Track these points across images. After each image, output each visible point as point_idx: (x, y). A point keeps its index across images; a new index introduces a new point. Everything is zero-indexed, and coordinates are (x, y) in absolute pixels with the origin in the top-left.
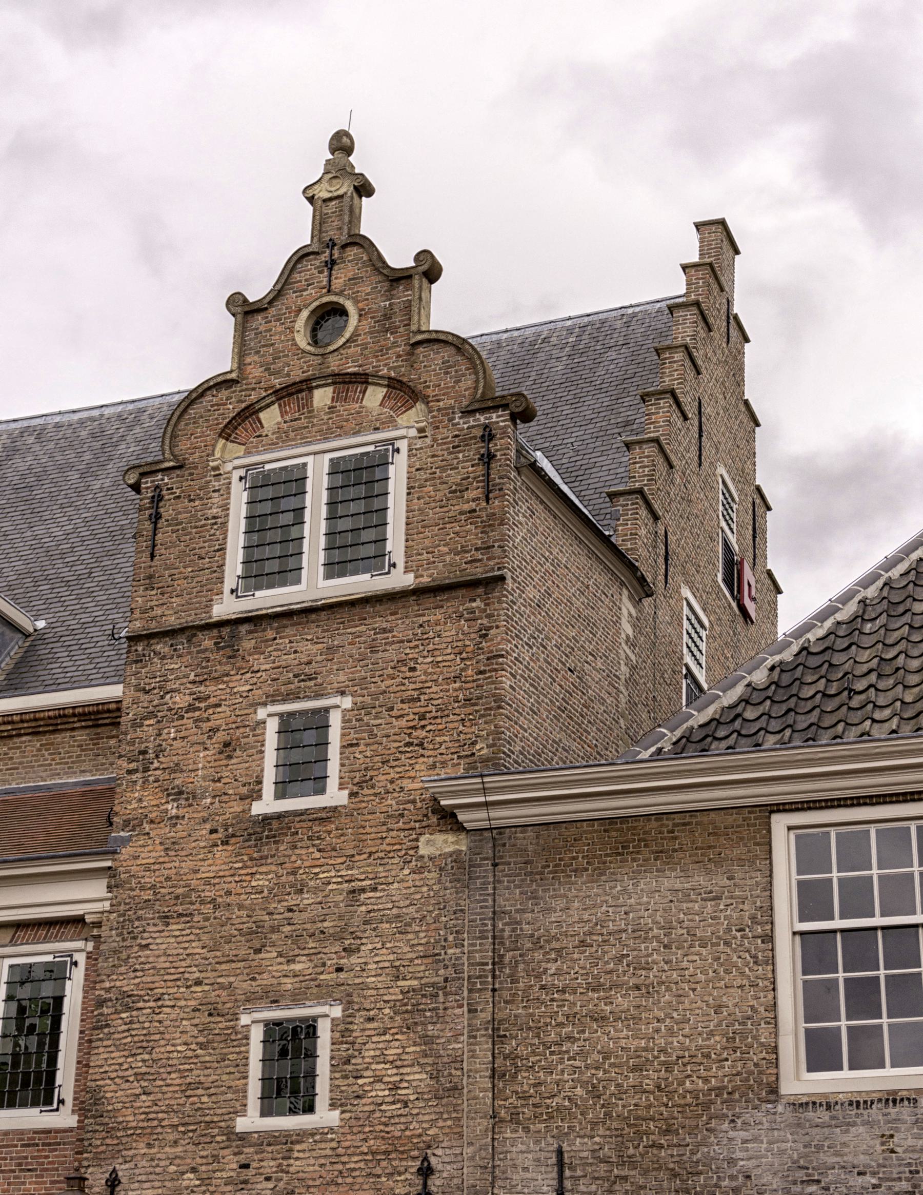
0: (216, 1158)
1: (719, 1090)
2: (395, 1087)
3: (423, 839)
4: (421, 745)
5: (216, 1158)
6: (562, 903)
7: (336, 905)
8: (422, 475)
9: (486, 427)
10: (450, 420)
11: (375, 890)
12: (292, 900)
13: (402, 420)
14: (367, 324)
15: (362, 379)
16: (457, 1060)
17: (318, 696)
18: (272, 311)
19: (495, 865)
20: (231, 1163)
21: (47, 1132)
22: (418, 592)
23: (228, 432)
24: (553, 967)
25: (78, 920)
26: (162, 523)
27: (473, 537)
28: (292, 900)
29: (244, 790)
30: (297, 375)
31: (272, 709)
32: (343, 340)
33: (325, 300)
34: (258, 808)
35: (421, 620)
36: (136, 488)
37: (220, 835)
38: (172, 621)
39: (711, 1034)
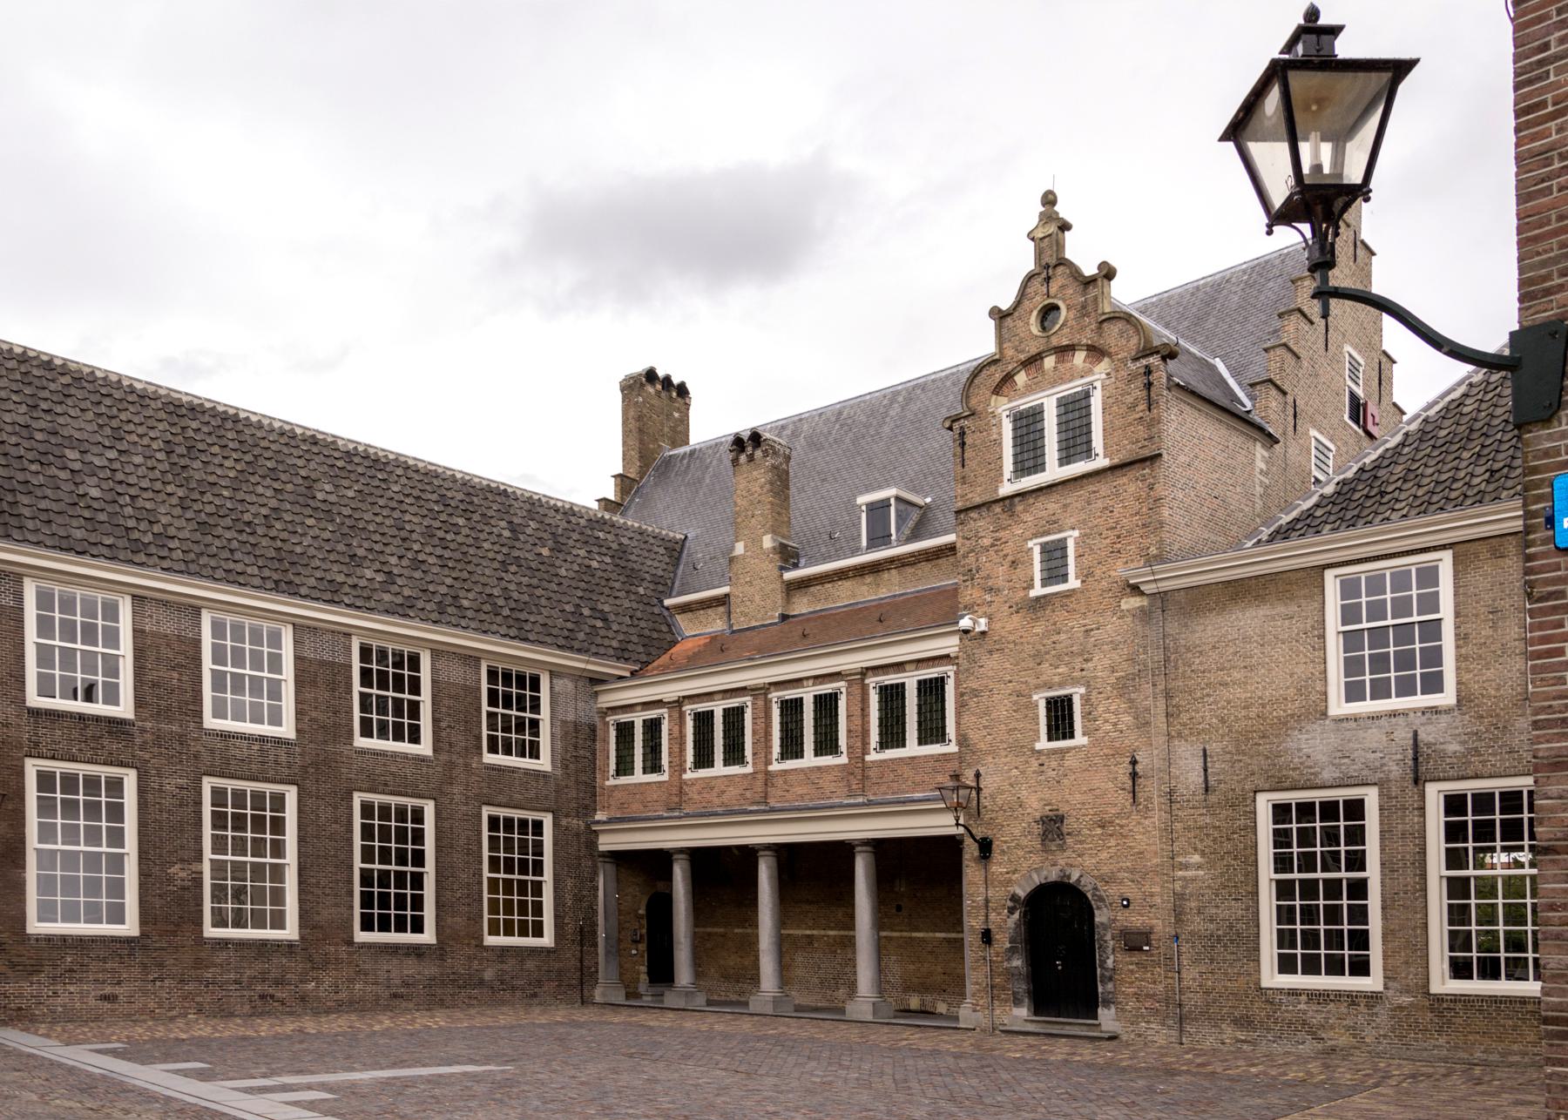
0: (1027, 762)
1: (1292, 716)
2: (1115, 724)
3: (1123, 601)
4: (1119, 552)
5: (1027, 762)
6: (1202, 627)
7: (1078, 638)
8: (1111, 400)
9: (1146, 367)
10: (1125, 365)
11: (1098, 629)
12: (1055, 638)
13: (1097, 369)
15: (1071, 348)
16: (1148, 710)
17: (1060, 531)
18: (1016, 314)
19: (1163, 611)
20: (1035, 764)
21: (945, 754)
22: (1112, 469)
23: (997, 390)
24: (1197, 661)
25: (947, 656)
26: (966, 447)
27: (1141, 431)
28: (1055, 638)
29: (1025, 585)
30: (1034, 351)
31: (1035, 541)
32: (1057, 327)
33: (1046, 302)
34: (1033, 593)
35: (1115, 484)
36: (950, 428)
37: (1015, 608)
38: (978, 500)
39: (1288, 688)
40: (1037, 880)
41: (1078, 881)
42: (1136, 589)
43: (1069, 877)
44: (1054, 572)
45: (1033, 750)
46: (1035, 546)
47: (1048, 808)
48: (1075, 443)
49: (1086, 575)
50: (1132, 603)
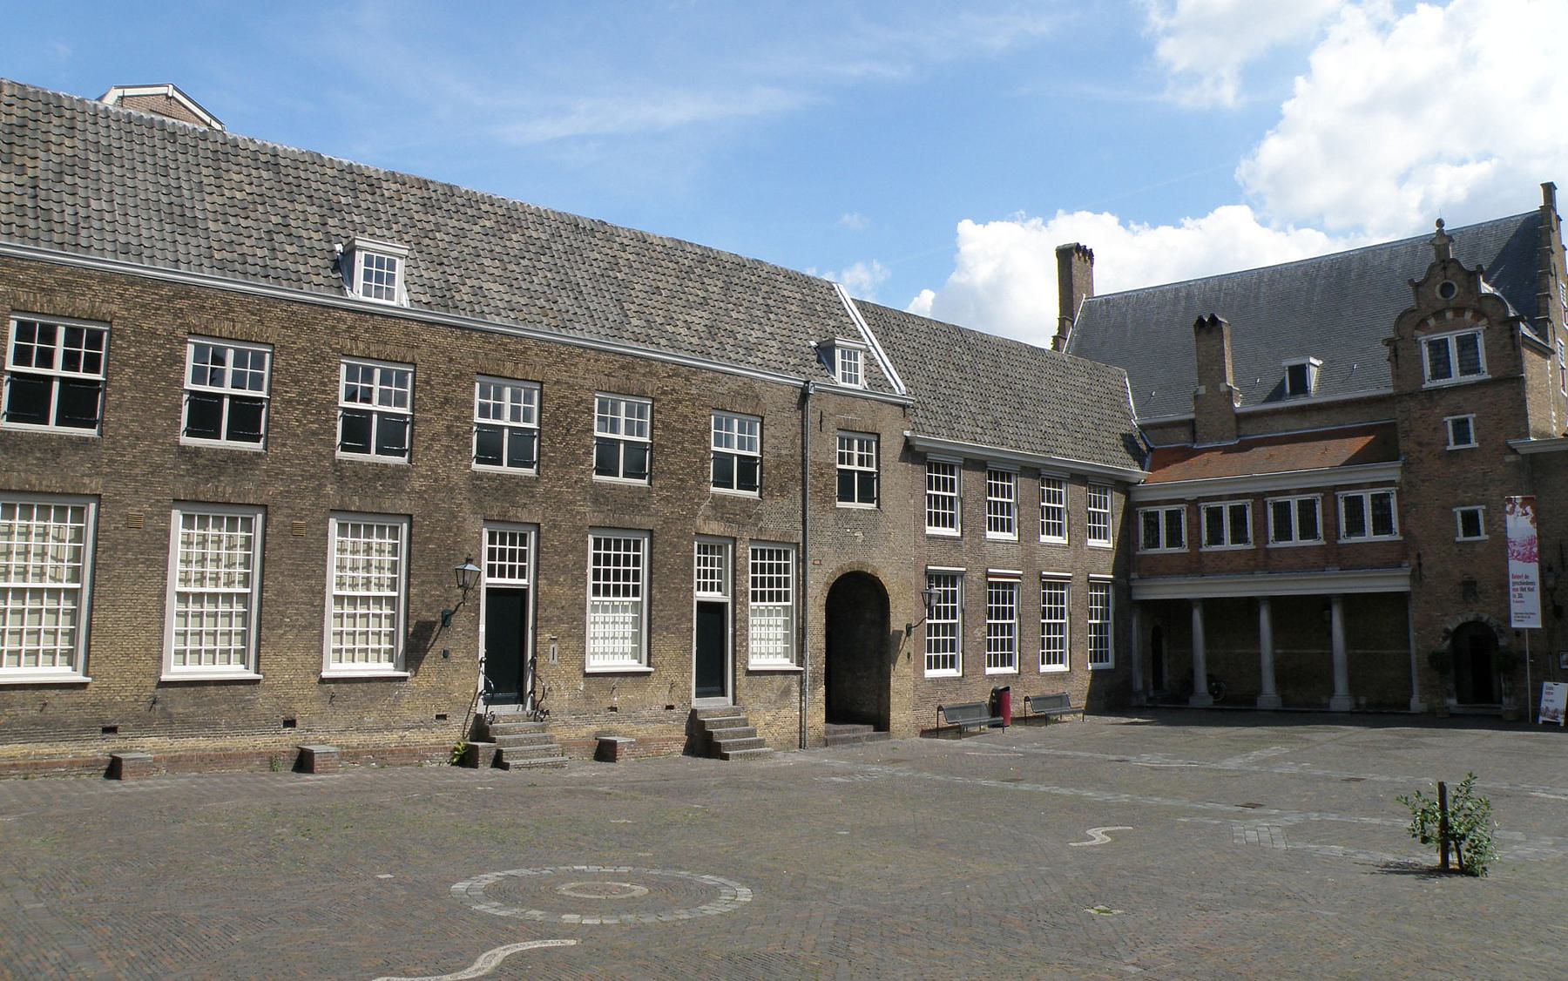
13: (1480, 323)
14: (1462, 290)
18: (1426, 285)
20: (1456, 550)
23: (1417, 327)
31: (1448, 418)
32: (1453, 296)
33: (1445, 281)
34: (1449, 448)
37: (1436, 457)
40: (1461, 620)
41: (1487, 621)
42: (1514, 451)
43: (1481, 618)
44: (1461, 435)
45: (1454, 541)
46: (1449, 420)
47: (1466, 576)
48: (1469, 366)
49: (1480, 439)
50: (1510, 458)
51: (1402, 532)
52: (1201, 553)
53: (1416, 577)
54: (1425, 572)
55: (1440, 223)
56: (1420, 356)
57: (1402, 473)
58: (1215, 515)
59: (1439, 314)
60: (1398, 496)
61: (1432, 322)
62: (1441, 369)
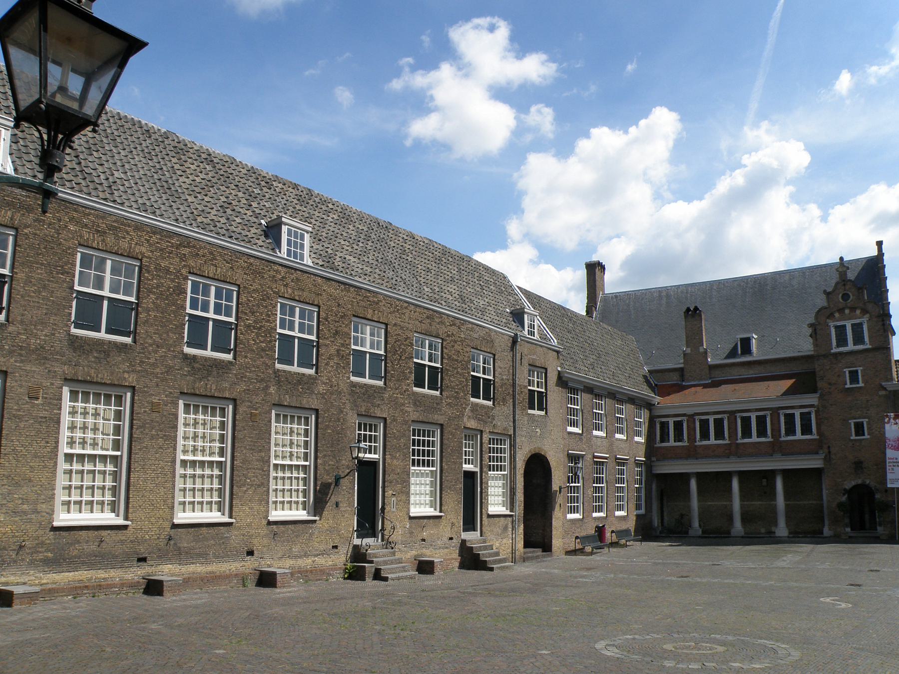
13: (865, 316)
17: (856, 367)
23: (828, 317)
34: (846, 386)
40: (853, 483)
41: (869, 484)
42: (885, 389)
46: (847, 370)
48: (858, 339)
50: (882, 393)
51: (819, 433)
52: (696, 446)
53: (828, 459)
54: (833, 457)
55: (841, 259)
56: (830, 335)
57: (819, 400)
58: (704, 424)
59: (841, 311)
60: (816, 414)
61: (837, 315)
62: (842, 341)
